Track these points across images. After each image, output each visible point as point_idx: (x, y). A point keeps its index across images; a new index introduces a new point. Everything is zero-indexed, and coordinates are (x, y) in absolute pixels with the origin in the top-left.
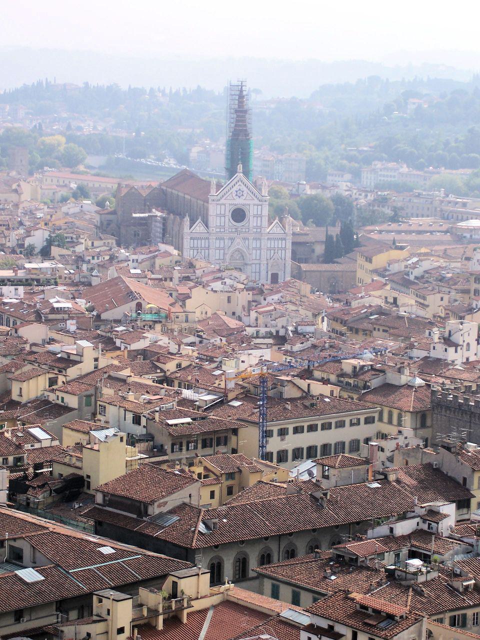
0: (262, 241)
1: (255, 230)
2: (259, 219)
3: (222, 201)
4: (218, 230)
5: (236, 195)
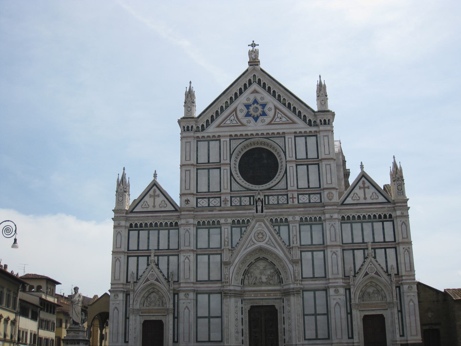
0: (327, 225)
1: (304, 199)
2: (313, 169)
3: (212, 130)
4: (203, 203)
5: (248, 115)
